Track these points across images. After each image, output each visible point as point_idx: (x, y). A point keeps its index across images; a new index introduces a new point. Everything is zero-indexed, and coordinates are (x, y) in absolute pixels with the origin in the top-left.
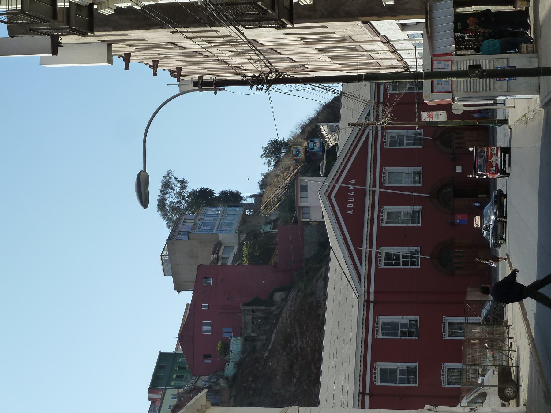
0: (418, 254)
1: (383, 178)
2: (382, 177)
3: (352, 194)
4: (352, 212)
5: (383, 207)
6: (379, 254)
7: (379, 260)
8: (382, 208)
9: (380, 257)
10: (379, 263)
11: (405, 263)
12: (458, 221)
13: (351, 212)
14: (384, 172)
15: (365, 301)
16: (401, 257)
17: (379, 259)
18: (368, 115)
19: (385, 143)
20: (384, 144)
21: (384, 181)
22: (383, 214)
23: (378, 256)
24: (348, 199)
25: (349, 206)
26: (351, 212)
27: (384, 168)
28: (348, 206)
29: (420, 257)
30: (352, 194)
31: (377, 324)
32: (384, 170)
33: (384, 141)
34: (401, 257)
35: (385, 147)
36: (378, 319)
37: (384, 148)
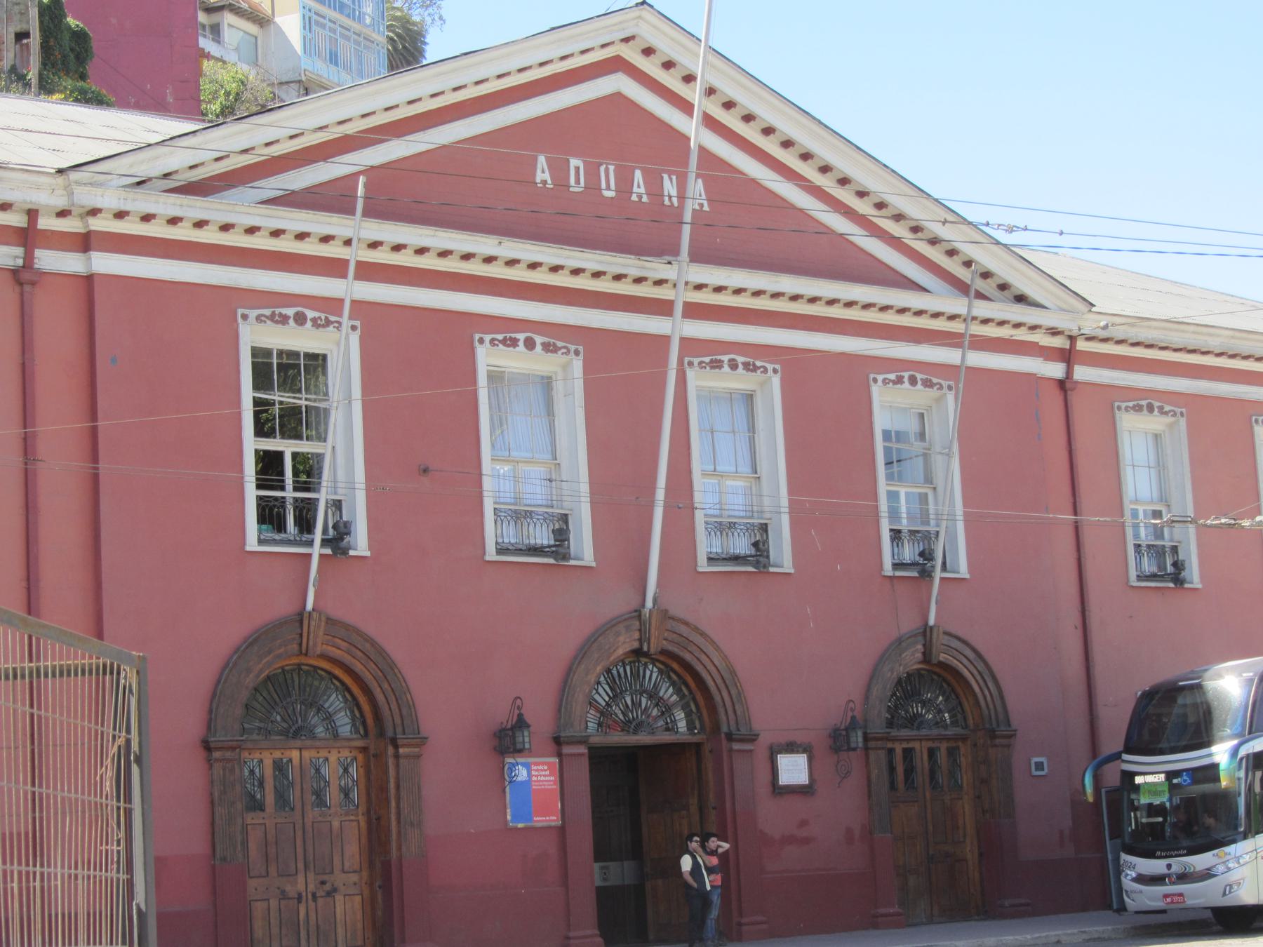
0: (325, 542)
2: (732, 356)
6: (316, 314)
7: (285, 311)
8: (573, 348)
9: (300, 319)
10: (267, 312)
11: (269, 464)
12: (522, 774)
13: (543, 174)
14: (755, 369)
15: (32, 214)
16: (304, 447)
17: (290, 312)
18: (1021, 299)
19: (895, 383)
20: (892, 376)
22: (539, 348)
24: (612, 168)
25: (577, 169)
26: (543, 174)
29: (310, 555)
32: (766, 370)
33: (906, 375)
34: (304, 447)
35: (875, 380)
37: (872, 376)
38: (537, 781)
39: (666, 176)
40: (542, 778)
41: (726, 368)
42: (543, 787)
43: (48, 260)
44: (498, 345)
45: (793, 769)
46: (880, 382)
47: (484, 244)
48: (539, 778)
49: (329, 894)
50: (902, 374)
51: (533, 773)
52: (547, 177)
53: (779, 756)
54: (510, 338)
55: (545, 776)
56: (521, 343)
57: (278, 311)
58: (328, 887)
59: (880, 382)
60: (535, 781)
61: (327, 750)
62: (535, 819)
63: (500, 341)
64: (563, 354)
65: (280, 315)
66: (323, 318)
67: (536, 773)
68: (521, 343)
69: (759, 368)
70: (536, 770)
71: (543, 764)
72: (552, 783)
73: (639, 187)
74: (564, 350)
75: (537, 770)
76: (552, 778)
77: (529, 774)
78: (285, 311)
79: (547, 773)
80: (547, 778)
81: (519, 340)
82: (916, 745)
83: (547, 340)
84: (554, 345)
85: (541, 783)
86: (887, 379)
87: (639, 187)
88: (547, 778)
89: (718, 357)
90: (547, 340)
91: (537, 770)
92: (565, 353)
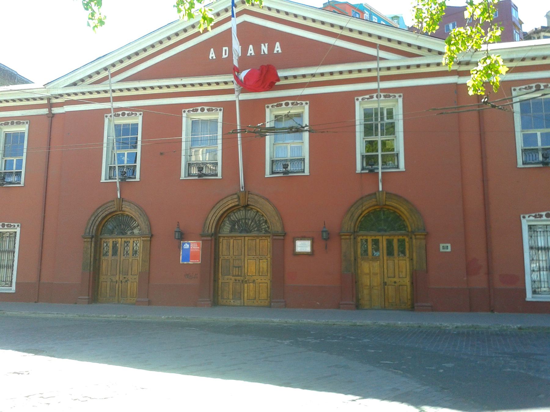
3: (249, 52)
4: (212, 57)
5: (220, 110)
6: (129, 112)
7: (118, 113)
8: (219, 109)
12: (186, 246)
13: (212, 55)
17: (120, 113)
21: (277, 106)
23: (125, 112)
25: (226, 50)
26: (212, 55)
28: (224, 48)
30: (251, 51)
31: (17, 123)
32: (302, 104)
36: (24, 123)
39: (262, 45)
40: (195, 248)
41: (284, 106)
42: (194, 251)
43: (56, 110)
44: (190, 112)
45: (446, 248)
47: (177, 81)
48: (193, 248)
49: (126, 281)
51: (191, 246)
52: (214, 55)
53: (297, 241)
56: (199, 110)
57: (116, 113)
58: (126, 279)
61: (130, 239)
62: (191, 261)
63: (191, 111)
64: (215, 111)
65: (117, 114)
66: (131, 113)
67: (193, 246)
68: (199, 110)
69: (299, 104)
70: (192, 245)
71: (195, 243)
73: (251, 50)
75: (193, 245)
76: (198, 248)
77: (190, 246)
78: (118, 113)
79: (197, 246)
80: (196, 248)
81: (198, 109)
83: (209, 107)
84: (212, 109)
87: (251, 50)
88: (196, 248)
89: (280, 103)
90: (209, 107)
91: (193, 245)
92: (216, 111)
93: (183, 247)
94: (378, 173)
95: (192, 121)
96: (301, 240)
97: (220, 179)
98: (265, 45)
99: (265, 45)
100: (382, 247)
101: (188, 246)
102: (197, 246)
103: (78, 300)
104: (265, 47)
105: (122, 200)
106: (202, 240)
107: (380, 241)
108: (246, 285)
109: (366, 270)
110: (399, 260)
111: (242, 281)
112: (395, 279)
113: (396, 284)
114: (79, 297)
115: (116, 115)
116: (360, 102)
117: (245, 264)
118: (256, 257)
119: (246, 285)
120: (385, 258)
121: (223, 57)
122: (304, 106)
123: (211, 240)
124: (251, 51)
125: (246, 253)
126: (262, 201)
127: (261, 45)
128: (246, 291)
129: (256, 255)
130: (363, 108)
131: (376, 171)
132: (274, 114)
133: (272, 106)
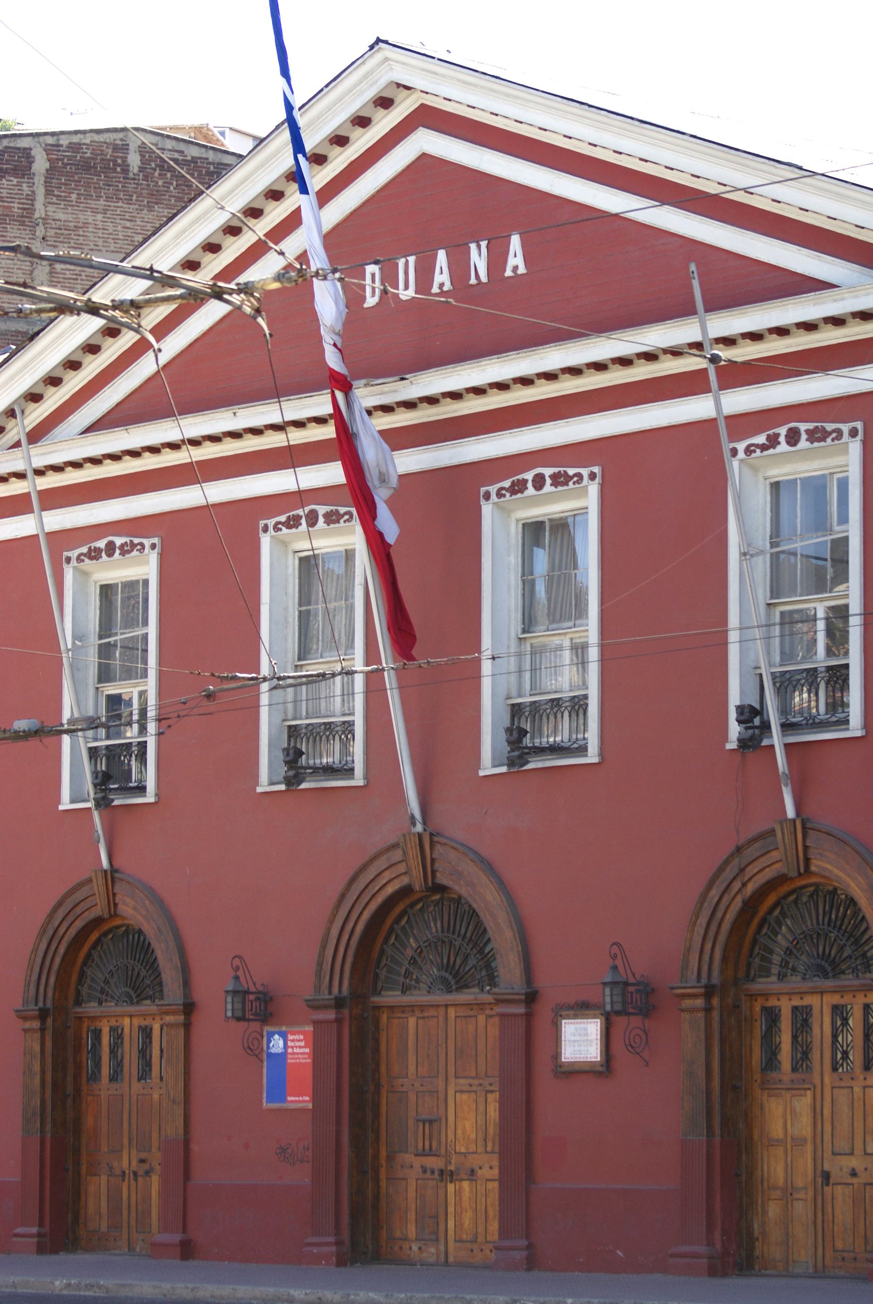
1: (529, 476)
12: (277, 1044)
14: (568, 478)
19: (763, 448)
20: (761, 439)
22: (321, 520)
24: (412, 259)
25: (373, 275)
27: (596, 469)
33: (783, 431)
38: (293, 1053)
41: (530, 490)
42: (298, 1061)
46: (741, 455)
48: (295, 1050)
50: (776, 431)
51: (290, 1044)
53: (563, 1021)
54: (293, 516)
55: (300, 1047)
57: (93, 545)
59: (741, 455)
60: (291, 1054)
61: (151, 1018)
62: (290, 1099)
64: (345, 522)
69: (571, 478)
70: (293, 1041)
71: (299, 1033)
72: (307, 1056)
74: (346, 517)
76: (307, 1050)
79: (303, 1044)
80: (302, 1050)
82: (812, 1000)
85: (296, 1056)
86: (752, 445)
88: (302, 1050)
89: (520, 477)
93: (268, 1047)
94: (773, 746)
95: (301, 559)
96: (575, 1017)
97: (360, 786)
98: (479, 247)
99: (479, 247)
100: (819, 1035)
101: (281, 1043)
102: (303, 1044)
103: (15, 1239)
104: (480, 255)
105: (112, 876)
106: (315, 1023)
107: (816, 1011)
108: (451, 1187)
109: (776, 1130)
110: (864, 1087)
111: (442, 1172)
112: (854, 1162)
113: (855, 1180)
114: (20, 1230)
115: (93, 554)
116: (741, 461)
117: (449, 1109)
118: (476, 1082)
119: (451, 1187)
120: (827, 1080)
121: (366, 306)
122: (587, 486)
123: (339, 1021)
124: (442, 278)
125: (451, 1069)
126: (469, 868)
127: (470, 247)
128: (451, 1209)
129: (477, 1077)
130: (768, 482)
131: (765, 742)
132: (518, 521)
133: (499, 495)
